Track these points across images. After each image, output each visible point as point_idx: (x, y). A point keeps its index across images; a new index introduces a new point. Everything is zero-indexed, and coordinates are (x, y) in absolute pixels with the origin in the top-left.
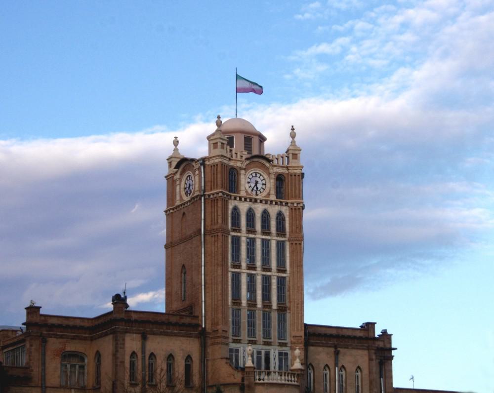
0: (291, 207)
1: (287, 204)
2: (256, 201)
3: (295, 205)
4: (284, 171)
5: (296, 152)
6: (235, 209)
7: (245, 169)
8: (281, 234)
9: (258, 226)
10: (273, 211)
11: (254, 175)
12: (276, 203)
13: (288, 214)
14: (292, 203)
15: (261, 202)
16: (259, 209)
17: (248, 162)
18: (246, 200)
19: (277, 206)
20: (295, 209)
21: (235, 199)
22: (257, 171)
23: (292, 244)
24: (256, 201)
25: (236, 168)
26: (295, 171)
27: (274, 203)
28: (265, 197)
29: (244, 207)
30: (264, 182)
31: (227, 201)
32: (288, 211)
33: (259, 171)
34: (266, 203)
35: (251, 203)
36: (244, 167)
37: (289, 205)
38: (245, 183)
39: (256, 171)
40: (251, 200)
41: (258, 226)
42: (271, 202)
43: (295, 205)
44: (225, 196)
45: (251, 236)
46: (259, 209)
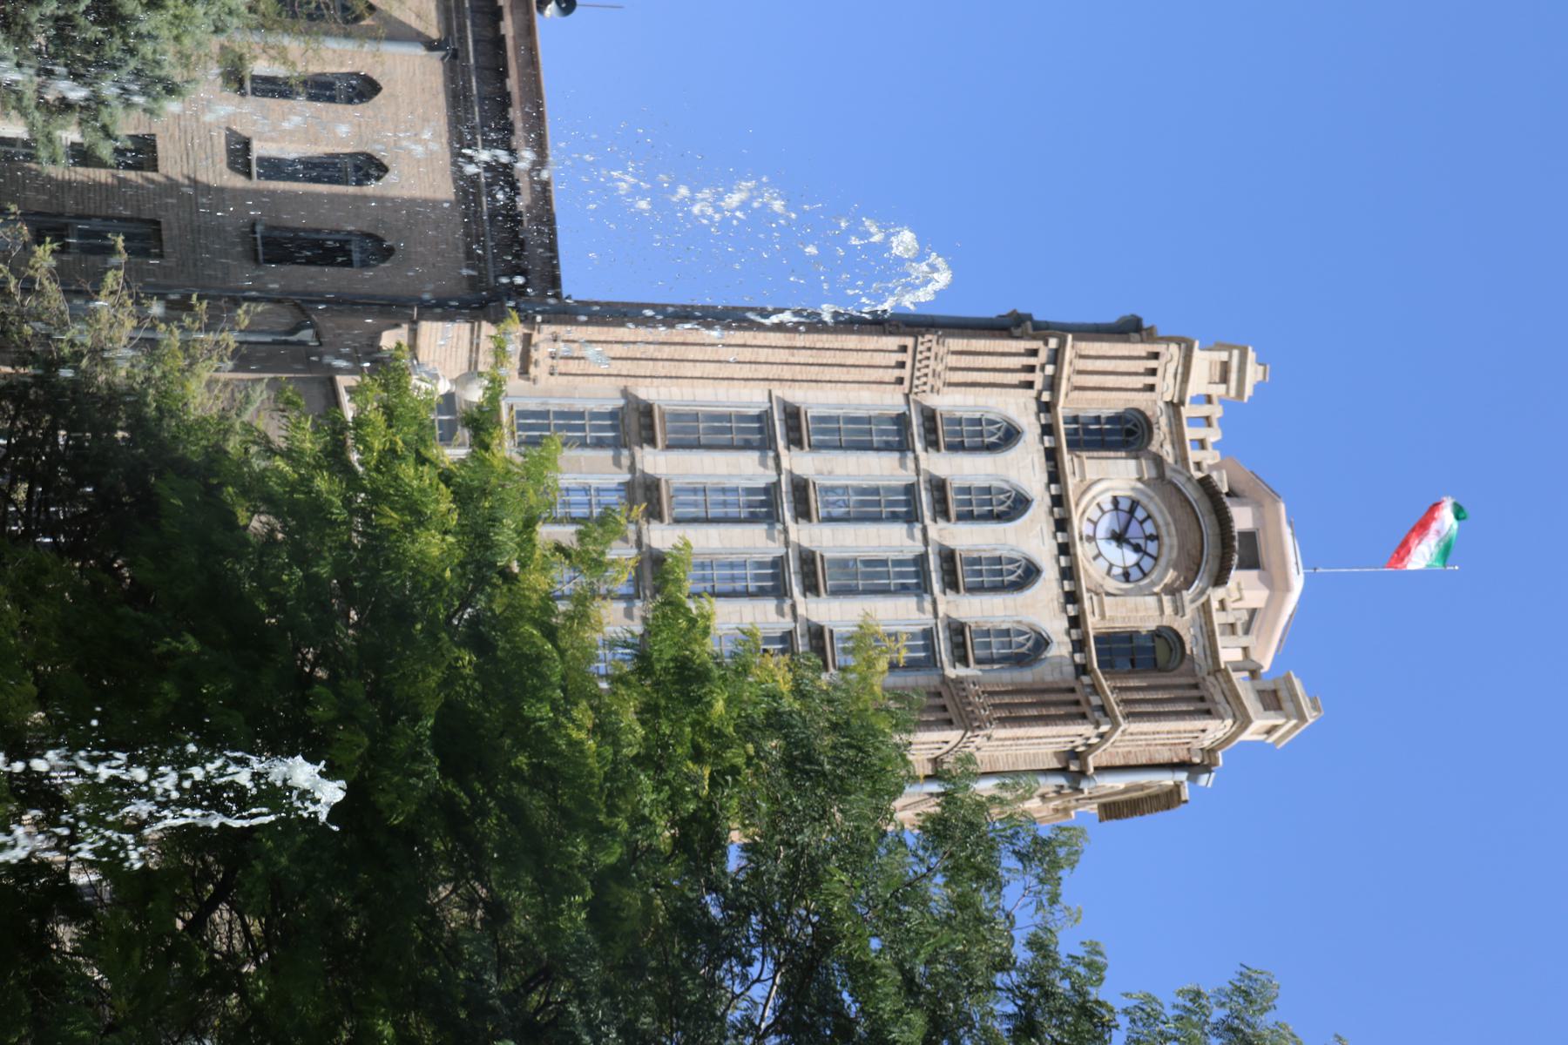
0: (1078, 687)
1: (1082, 669)
2: (1062, 525)
3: (1095, 700)
4: (1203, 665)
5: (1288, 706)
6: (1010, 435)
7: (1161, 476)
8: (964, 645)
9: (968, 538)
10: (1039, 608)
11: (1149, 528)
12: (1076, 622)
13: (1049, 678)
14: (1095, 689)
15: (1065, 549)
16: (1031, 537)
17: (1192, 493)
18: (1055, 476)
19: (1066, 624)
20: (1077, 703)
21: (1048, 430)
22: (1166, 540)
23: (939, 695)
24: (1062, 525)
25: (1156, 437)
26: (1219, 697)
27: (1072, 610)
28: (1086, 571)
29: (1023, 468)
30: (1135, 573)
31: (1030, 385)
32: (1057, 676)
33: (1171, 547)
34: (1069, 573)
35: (1048, 501)
36: (1169, 474)
37: (1086, 679)
38: (1110, 478)
39: (1163, 531)
40: (1058, 501)
41: (968, 538)
42: (1072, 597)
43: (1095, 700)
44: (1050, 369)
45: (925, 497)
46: (1031, 537)
